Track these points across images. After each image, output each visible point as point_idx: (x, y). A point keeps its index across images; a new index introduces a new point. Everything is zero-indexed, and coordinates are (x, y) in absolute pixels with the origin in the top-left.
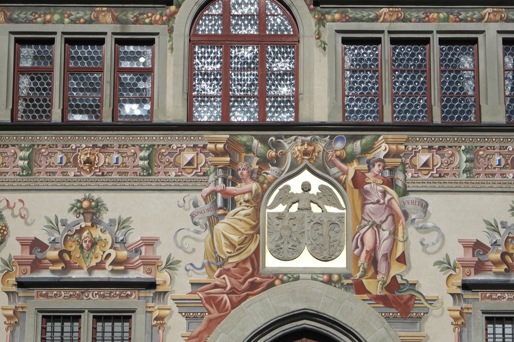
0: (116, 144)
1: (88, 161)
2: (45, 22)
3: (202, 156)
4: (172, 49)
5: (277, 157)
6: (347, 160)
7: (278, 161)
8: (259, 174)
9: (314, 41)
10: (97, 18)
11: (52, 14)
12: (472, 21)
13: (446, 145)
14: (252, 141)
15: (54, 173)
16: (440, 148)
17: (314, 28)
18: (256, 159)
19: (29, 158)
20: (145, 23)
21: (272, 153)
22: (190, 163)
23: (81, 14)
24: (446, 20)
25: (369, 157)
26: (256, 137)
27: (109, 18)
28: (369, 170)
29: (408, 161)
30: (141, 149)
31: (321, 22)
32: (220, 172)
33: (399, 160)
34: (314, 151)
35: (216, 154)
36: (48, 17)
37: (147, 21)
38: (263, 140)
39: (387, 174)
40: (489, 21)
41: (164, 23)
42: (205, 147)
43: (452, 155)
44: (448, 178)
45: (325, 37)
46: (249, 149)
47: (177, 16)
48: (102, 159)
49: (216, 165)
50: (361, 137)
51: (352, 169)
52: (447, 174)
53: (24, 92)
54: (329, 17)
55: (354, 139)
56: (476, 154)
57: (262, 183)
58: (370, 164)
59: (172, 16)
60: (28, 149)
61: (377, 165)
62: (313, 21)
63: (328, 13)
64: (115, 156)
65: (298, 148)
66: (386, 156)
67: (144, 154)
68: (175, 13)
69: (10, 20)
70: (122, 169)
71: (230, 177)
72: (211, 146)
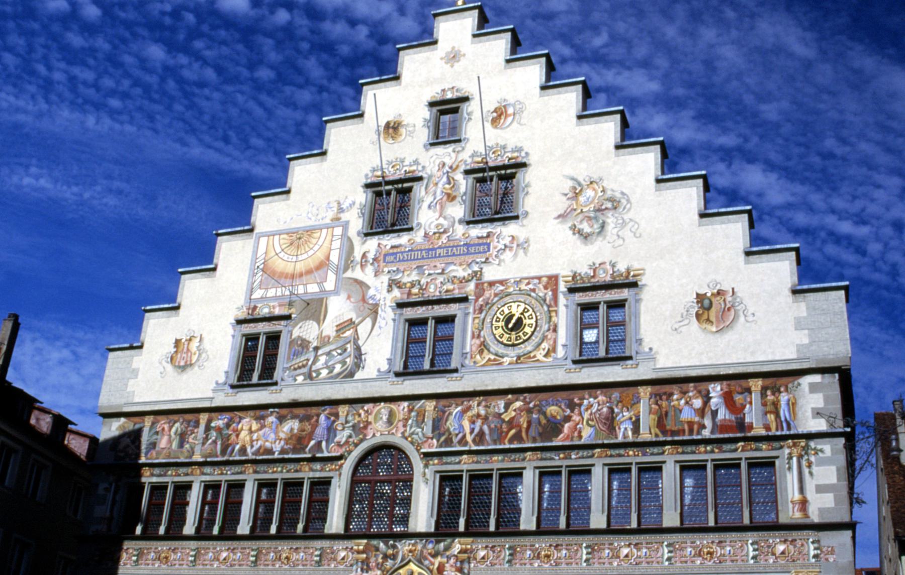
0: (303, 547)
1: (287, 558)
2: (273, 472)
3: (350, 554)
4: (339, 486)
5: (393, 555)
6: (434, 556)
7: (394, 557)
8: (382, 565)
9: (421, 478)
10: (300, 469)
11: (277, 467)
12: (518, 461)
13: (496, 544)
14: (379, 544)
15: (268, 565)
16: (493, 547)
17: (422, 470)
18: (381, 556)
19: (256, 556)
20: (326, 471)
21: (390, 551)
22: (343, 559)
23: (292, 467)
24: (503, 461)
25: (448, 553)
26: (383, 542)
27: (307, 469)
28: (447, 562)
29: (472, 555)
30: (316, 550)
31: (426, 466)
32: (360, 564)
33: (466, 555)
34: (415, 550)
35: (359, 552)
36: (275, 469)
37: (327, 469)
38: (386, 544)
39: (458, 564)
40: (530, 460)
41: (336, 470)
42: (352, 548)
43: (500, 551)
44: (496, 566)
45: (428, 476)
46: (377, 549)
47: (344, 466)
48: (294, 556)
49: (357, 560)
50: (444, 541)
51: (437, 561)
52: (496, 564)
53: (260, 515)
54: (431, 462)
55: (438, 542)
56: (515, 550)
57: (383, 571)
58: (449, 558)
59: (341, 466)
60: (256, 550)
61: (452, 558)
62: (422, 466)
63: (431, 460)
64: (302, 554)
65: (407, 548)
66: (459, 553)
67: (317, 553)
68: (343, 464)
69: (255, 472)
70: (305, 563)
71: (365, 567)
72: (355, 548)
